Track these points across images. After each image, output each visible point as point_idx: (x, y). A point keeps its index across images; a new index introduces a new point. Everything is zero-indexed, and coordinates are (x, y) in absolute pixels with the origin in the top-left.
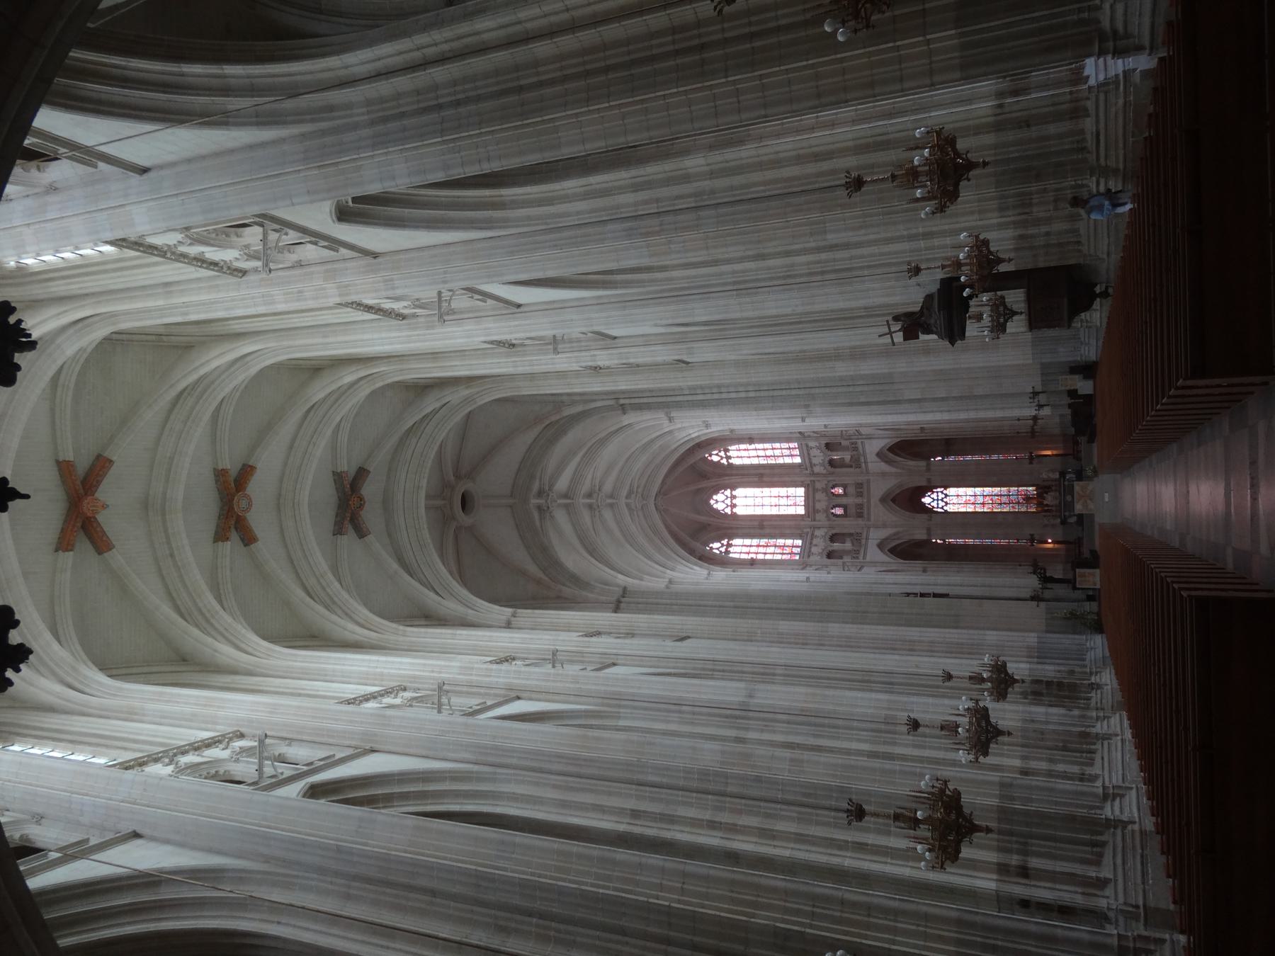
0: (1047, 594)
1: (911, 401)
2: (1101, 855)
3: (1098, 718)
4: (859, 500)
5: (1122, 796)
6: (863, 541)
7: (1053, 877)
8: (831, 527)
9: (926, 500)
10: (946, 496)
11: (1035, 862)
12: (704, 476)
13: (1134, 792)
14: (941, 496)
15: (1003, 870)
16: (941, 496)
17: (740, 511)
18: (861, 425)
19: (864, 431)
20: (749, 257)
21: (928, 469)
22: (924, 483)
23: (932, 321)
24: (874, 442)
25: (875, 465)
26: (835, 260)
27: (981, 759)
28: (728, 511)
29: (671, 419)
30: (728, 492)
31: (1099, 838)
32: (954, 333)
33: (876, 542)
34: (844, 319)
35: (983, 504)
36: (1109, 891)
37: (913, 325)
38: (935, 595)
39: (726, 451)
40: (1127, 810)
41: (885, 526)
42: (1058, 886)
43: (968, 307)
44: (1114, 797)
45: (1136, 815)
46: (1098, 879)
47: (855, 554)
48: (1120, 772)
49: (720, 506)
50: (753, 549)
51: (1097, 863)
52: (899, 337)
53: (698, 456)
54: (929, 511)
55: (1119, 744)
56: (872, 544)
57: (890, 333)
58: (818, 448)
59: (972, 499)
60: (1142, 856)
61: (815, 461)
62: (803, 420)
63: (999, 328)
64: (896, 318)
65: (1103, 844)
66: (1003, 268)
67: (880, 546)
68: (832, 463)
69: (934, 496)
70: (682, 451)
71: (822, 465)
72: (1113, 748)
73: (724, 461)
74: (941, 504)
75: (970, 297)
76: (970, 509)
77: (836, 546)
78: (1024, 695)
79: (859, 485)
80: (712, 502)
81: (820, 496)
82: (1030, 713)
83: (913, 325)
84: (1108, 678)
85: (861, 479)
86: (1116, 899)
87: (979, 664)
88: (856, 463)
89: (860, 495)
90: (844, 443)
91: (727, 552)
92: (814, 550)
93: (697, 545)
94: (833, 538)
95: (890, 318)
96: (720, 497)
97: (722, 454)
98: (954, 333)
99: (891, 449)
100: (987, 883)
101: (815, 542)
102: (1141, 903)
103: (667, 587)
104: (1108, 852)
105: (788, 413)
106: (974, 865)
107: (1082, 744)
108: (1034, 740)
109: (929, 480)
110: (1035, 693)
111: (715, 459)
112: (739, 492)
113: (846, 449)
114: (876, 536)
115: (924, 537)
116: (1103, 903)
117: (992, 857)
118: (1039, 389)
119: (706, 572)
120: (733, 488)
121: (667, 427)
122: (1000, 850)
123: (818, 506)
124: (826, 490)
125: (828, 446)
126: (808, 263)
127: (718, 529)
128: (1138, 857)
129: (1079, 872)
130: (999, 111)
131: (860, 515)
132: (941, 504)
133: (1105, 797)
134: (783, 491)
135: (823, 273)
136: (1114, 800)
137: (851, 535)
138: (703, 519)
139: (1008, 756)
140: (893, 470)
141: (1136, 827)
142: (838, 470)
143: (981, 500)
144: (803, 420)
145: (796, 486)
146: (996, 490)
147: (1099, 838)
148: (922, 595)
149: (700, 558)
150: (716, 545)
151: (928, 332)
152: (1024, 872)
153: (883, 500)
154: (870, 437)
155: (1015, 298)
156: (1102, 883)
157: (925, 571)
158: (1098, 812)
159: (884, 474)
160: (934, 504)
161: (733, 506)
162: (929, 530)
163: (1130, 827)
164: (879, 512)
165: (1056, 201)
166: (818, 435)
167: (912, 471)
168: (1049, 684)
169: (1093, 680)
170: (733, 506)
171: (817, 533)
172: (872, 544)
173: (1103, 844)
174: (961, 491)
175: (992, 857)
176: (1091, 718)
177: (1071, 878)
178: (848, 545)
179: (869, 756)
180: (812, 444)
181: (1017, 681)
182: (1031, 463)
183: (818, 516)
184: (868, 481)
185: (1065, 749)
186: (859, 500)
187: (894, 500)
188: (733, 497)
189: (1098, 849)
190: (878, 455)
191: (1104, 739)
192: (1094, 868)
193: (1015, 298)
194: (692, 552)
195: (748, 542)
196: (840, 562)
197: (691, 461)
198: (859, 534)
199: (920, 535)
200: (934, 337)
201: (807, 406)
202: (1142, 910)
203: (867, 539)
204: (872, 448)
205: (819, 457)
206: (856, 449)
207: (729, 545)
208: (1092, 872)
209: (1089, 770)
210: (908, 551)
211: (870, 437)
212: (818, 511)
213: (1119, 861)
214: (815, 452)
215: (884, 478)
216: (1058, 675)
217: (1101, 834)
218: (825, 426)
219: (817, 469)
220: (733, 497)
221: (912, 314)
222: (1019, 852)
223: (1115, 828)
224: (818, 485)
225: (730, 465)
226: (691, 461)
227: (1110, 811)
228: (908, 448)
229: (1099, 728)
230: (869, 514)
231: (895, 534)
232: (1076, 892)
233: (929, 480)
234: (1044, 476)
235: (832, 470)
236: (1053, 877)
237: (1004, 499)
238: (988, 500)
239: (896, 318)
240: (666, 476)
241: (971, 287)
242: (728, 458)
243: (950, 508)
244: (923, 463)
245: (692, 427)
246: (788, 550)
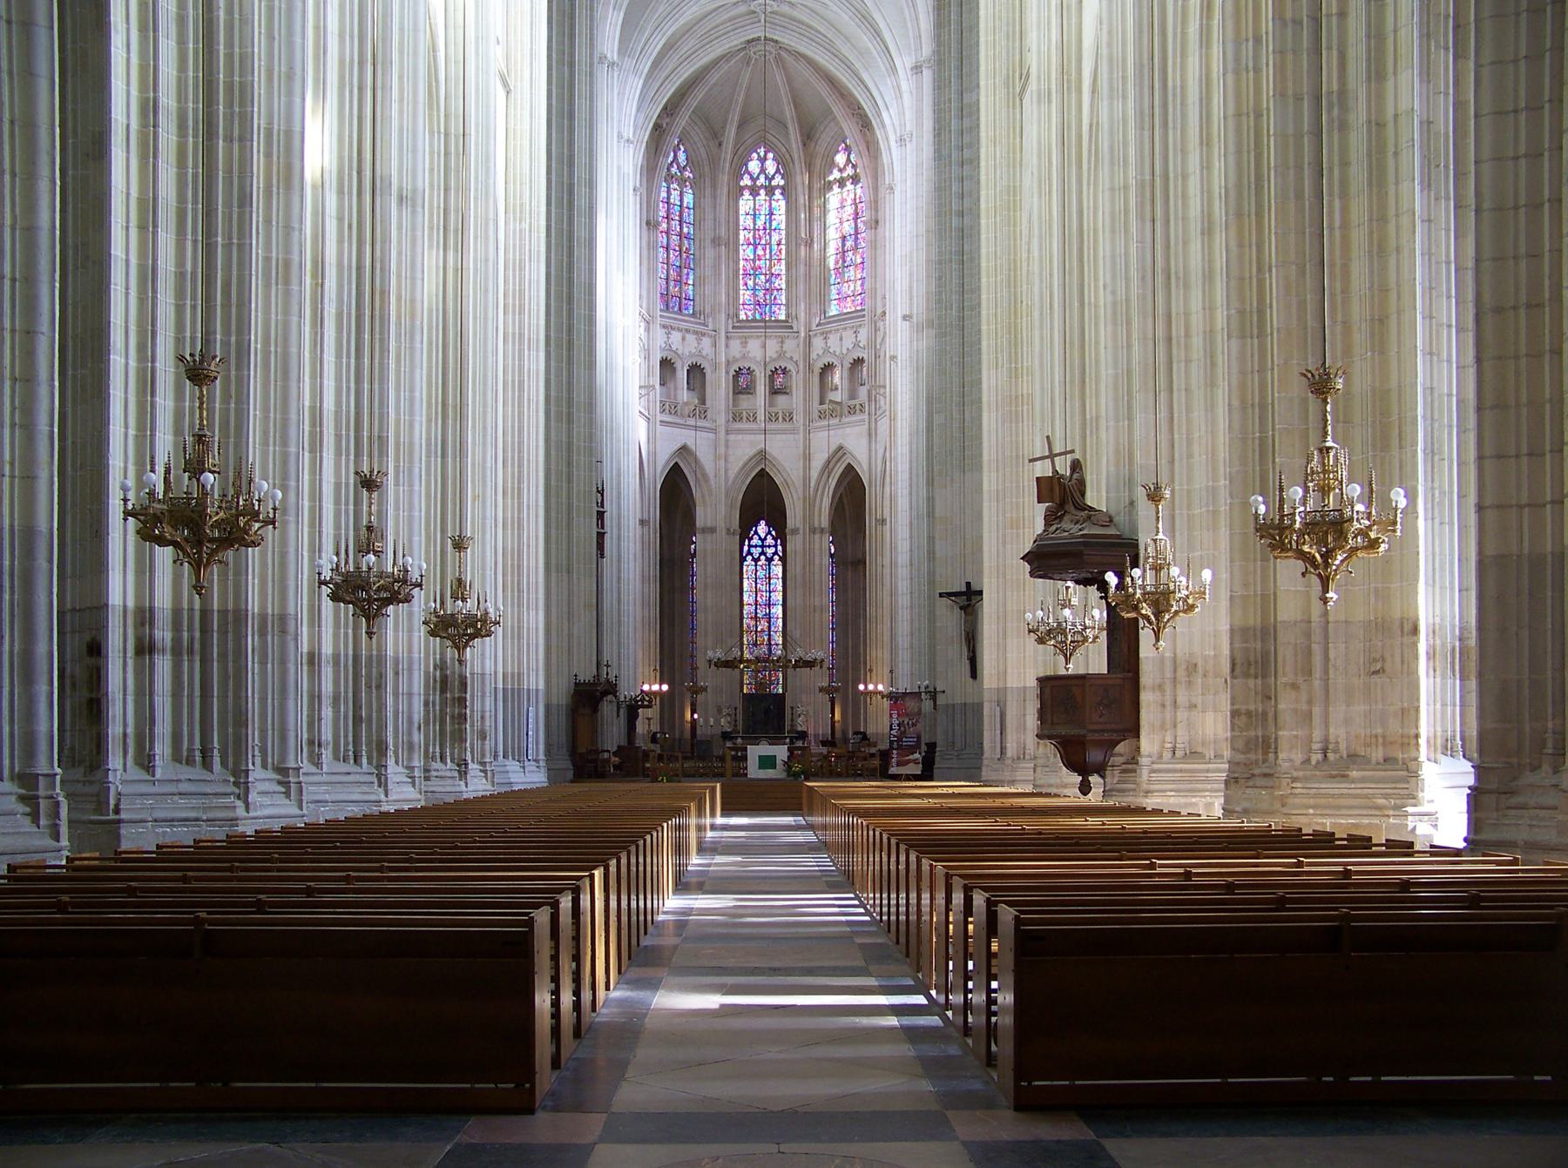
0: (607, 708)
1: (930, 500)
2: (190, 762)
3: (411, 768)
4: (761, 416)
5: (287, 794)
6: (691, 422)
7: (145, 691)
8: (715, 367)
9: (762, 528)
10: (770, 560)
11: (163, 665)
12: (808, 136)
13: (296, 811)
14: (770, 551)
15: (144, 616)
16: (770, 551)
17: (746, 203)
18: (893, 419)
19: (883, 425)
20: (1210, 205)
21: (813, 531)
22: (790, 523)
23: (1066, 524)
24: (864, 441)
25: (823, 443)
26: (1188, 361)
27: (326, 590)
28: (746, 181)
29: (917, 69)
30: (778, 181)
31: (217, 760)
32: (1046, 560)
33: (691, 444)
34: (1079, 377)
35: (756, 618)
36: (135, 773)
37: (1062, 494)
38: (601, 536)
39: (855, 179)
40: (266, 800)
41: (716, 457)
42: (130, 699)
43: (1085, 582)
44: (286, 784)
45: (259, 813)
46: (151, 757)
47: (670, 406)
48: (327, 797)
49: (754, 166)
50: (676, 224)
51: (177, 757)
52: (1043, 469)
53: (850, 128)
54: (745, 535)
55: (373, 798)
56: (684, 437)
57: (1052, 456)
58: (856, 345)
60: (197, 820)
61: (833, 340)
62: (905, 318)
63: (1048, 634)
64: (1076, 466)
65: (207, 764)
66: (1146, 635)
67: (684, 450)
68: (828, 368)
69: (770, 541)
70: (858, 94)
71: (826, 351)
72: (365, 788)
73: (836, 175)
74: (756, 552)
75: (1103, 587)
77: (682, 375)
78: (442, 666)
79: (789, 417)
80: (762, 151)
81: (772, 347)
82: (410, 669)
83: (1062, 494)
84: (477, 786)
85: (799, 418)
86: (123, 782)
87: (488, 591)
88: (832, 412)
89: (772, 418)
90: (863, 392)
91: (670, 178)
92: (676, 337)
93: (682, 120)
94: (696, 372)
95: (1077, 456)
96: (771, 167)
97: (849, 171)
98: (1046, 560)
99: (850, 468)
100: (120, 590)
101: (691, 338)
102: (123, 816)
103: (603, 58)
104: (197, 772)
105: (921, 290)
106: (145, 570)
107: (366, 742)
108: (366, 677)
109: (795, 531)
110: (444, 680)
111: (840, 159)
112: (780, 205)
113: (853, 396)
114: (701, 444)
115: (699, 523)
116: (115, 761)
117: (163, 599)
118: (941, 700)
119: (629, 132)
120: (785, 191)
121: (904, 63)
122: (177, 612)
123: (754, 347)
124: (781, 355)
125: (859, 362)
126: (1187, 315)
127: (714, 162)
128: (193, 815)
129: (158, 729)
130: (1407, 627)
131: (737, 417)
132: (756, 552)
133: (282, 771)
134: (781, 283)
135: (1169, 339)
136: (279, 783)
137: (703, 401)
138: (731, 133)
139: (336, 636)
140: (815, 474)
141: (241, 812)
142: (816, 380)
144: (905, 318)
145: (787, 305)
147: (217, 760)
148: (601, 515)
149: (657, 126)
150: (682, 157)
151: (1050, 518)
152: (145, 648)
153: (762, 455)
154: (871, 434)
155: (1094, 660)
156: (146, 762)
157: (642, 522)
158: (258, 760)
159: (807, 458)
160: (755, 541)
161: (754, 192)
162: (712, 530)
163: (239, 803)
164: (744, 447)
165: (1249, 714)
166: (875, 346)
167: (807, 505)
168: (462, 701)
169: (473, 767)
170: (754, 192)
171: (706, 342)
172: (684, 437)
173: (207, 764)
175: (163, 599)
176: (410, 759)
177: (146, 718)
178: (684, 395)
179: (313, 408)
180: (863, 335)
181: (460, 648)
183: (736, 345)
184: (794, 431)
185: (357, 720)
186: (761, 416)
187: (763, 474)
188: (770, 191)
189: (198, 759)
190: (841, 448)
191: (379, 776)
192: (168, 751)
193: (1094, 660)
194: (670, 110)
195: (689, 216)
196: (656, 380)
197: (838, 110)
198: (704, 414)
199: (702, 517)
200: (1039, 527)
201: (930, 324)
202: (112, 817)
203: (696, 428)
204: (853, 439)
205: (840, 345)
206: (852, 411)
207: (682, 182)
208: (162, 749)
209: (327, 755)
210: (676, 492)
211: (871, 434)
212: (744, 344)
213: (184, 787)
214: (849, 341)
215: (800, 458)
216: (477, 716)
217: (224, 764)
218: (893, 358)
219: (818, 343)
220: (770, 191)
221: (1083, 495)
222: (177, 641)
223: (235, 784)
224: (790, 345)
225: (828, 186)
226: (838, 110)
227: (259, 776)
228: (851, 498)
229: (394, 771)
230: (740, 431)
231: (704, 475)
232: (125, 725)
233: (795, 531)
235: (817, 371)
236: (145, 691)
238: (763, 625)
239: (1076, 466)
240: (810, 62)
241: (1121, 586)
242: (841, 183)
244: (825, 523)
245: (902, 113)
246: (674, 290)
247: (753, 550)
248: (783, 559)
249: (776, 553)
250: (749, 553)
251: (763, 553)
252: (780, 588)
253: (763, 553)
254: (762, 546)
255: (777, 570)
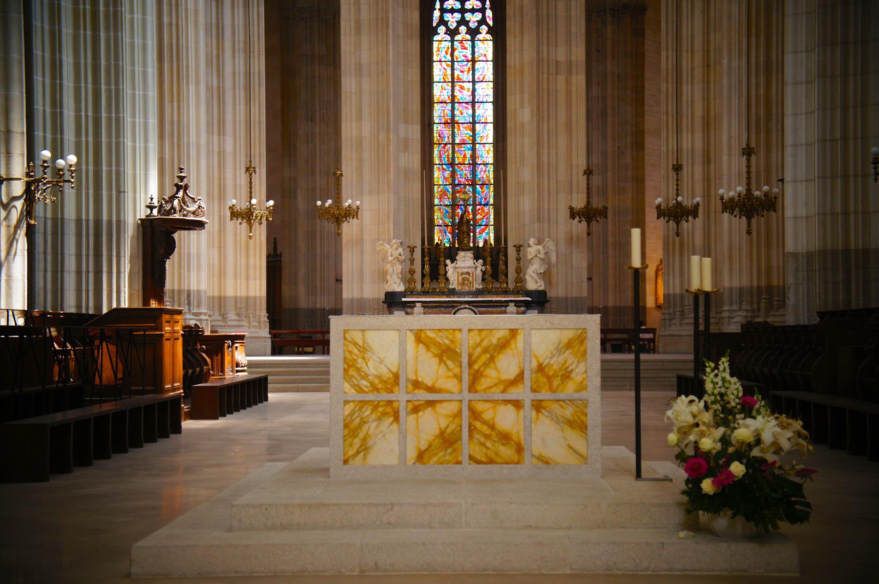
10: (473, 33)
14: (473, 19)
16: (473, 19)
35: (452, 123)
59: (464, 95)
74: (452, 20)
76: (440, 92)
132: (452, 20)
143: (463, 114)
146: (486, 154)
174: (486, 70)
182: (573, 213)
234: (532, 250)
237: (464, 173)
238: (463, 133)
243: (440, 44)
247: (447, 17)
248: (499, 34)
249: (483, 21)
250: (442, 22)
251: (463, 22)
252: (490, 76)
253: (463, 22)
254: (463, 11)
255: (486, 47)
